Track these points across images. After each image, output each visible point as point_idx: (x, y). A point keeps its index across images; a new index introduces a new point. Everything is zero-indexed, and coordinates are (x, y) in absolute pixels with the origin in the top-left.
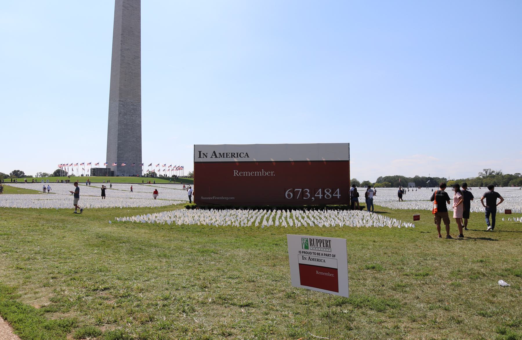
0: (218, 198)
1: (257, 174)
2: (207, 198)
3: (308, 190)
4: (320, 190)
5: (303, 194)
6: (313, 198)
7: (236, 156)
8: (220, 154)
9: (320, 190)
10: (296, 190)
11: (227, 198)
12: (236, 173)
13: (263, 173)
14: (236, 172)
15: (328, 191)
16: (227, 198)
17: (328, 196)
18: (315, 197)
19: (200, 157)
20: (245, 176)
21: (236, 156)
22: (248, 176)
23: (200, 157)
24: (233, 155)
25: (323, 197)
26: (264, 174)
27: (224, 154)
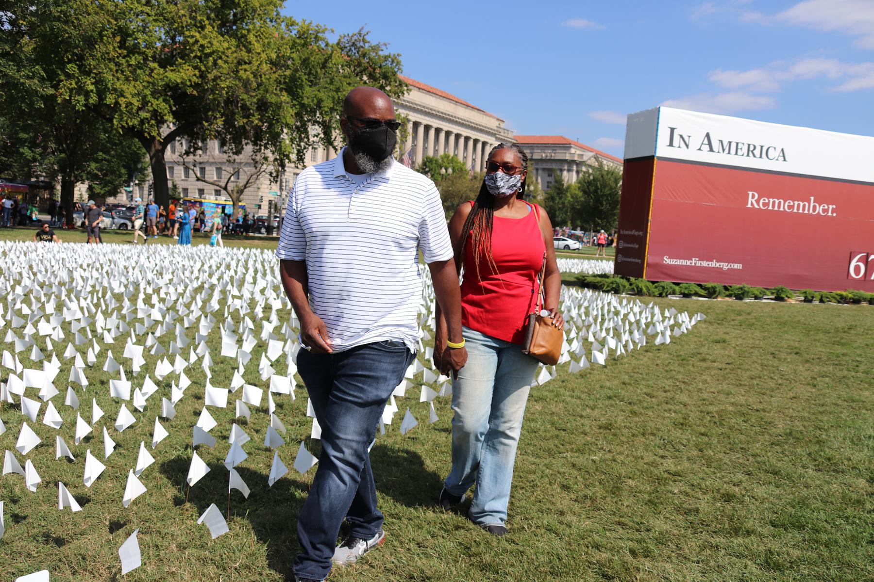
0: (705, 264)
2: (679, 262)
8: (721, 141)
11: (725, 266)
12: (752, 200)
14: (753, 196)
16: (725, 266)
19: (671, 144)
22: (778, 211)
23: (671, 144)
24: (750, 151)
26: (814, 208)
27: (730, 143)
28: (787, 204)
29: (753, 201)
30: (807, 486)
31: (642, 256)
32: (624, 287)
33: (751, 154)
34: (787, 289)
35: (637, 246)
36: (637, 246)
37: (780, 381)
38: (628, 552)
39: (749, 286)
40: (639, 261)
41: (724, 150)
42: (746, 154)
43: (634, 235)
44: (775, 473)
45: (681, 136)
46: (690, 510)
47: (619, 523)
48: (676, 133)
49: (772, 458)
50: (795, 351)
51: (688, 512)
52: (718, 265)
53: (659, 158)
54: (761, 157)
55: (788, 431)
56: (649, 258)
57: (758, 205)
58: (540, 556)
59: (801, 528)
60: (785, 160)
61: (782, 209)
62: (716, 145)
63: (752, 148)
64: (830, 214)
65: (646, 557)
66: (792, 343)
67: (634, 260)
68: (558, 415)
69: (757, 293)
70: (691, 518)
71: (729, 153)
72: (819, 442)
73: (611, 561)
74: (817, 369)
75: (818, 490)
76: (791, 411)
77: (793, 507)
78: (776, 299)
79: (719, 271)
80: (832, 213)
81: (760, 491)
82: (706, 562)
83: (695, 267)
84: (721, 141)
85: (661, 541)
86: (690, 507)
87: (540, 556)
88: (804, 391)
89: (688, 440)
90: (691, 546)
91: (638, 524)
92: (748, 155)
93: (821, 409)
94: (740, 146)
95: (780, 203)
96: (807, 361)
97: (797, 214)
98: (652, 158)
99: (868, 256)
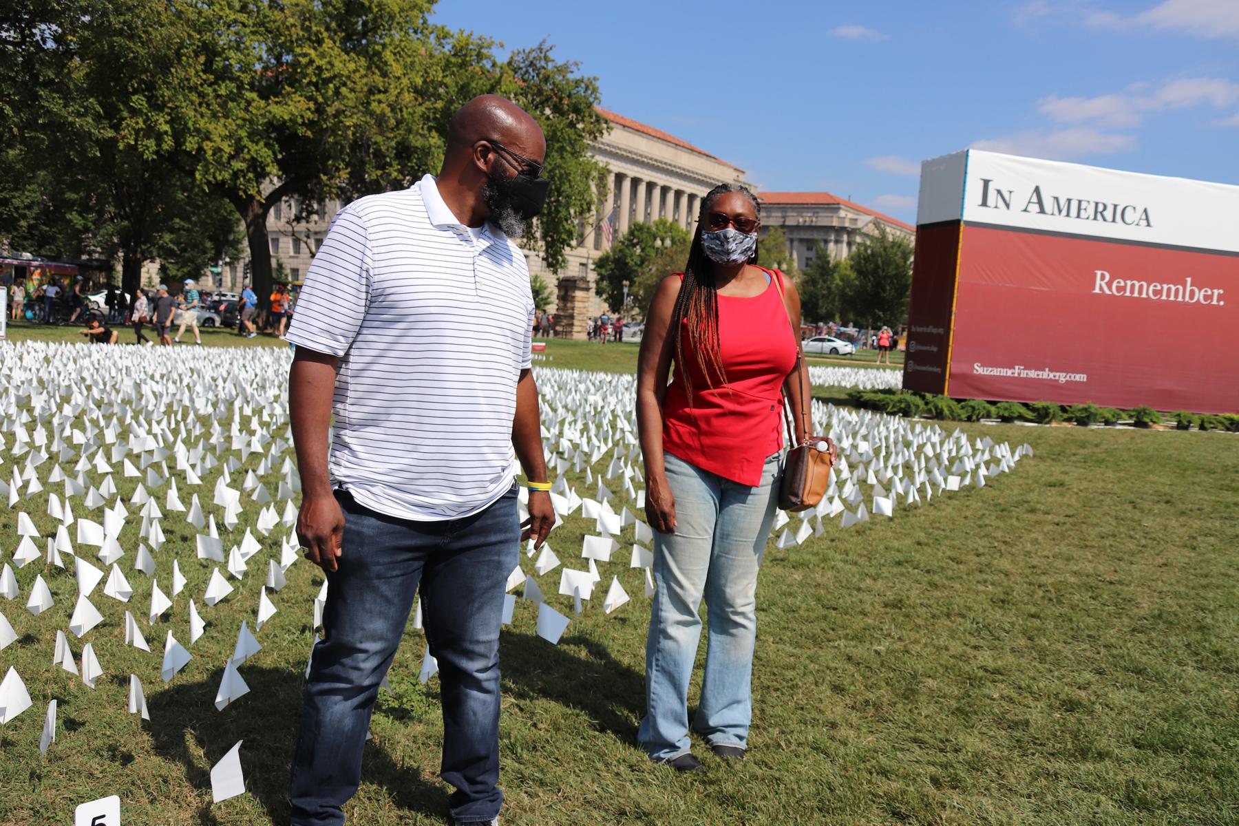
0: (1033, 374)
2: (996, 372)
7: (1108, 214)
8: (1057, 199)
11: (1062, 377)
12: (1102, 283)
13: (1189, 293)
14: (1103, 278)
16: (1062, 377)
19: (984, 203)
21: (1108, 214)
23: (984, 203)
24: (1099, 212)
27: (1069, 201)
28: (1151, 288)
30: (1186, 691)
31: (943, 365)
32: (917, 407)
33: (1099, 216)
34: (1153, 410)
35: (935, 349)
36: (935, 349)
37: (1143, 542)
38: (928, 781)
39: (1096, 406)
40: (939, 370)
41: (1060, 211)
42: (1092, 217)
43: (931, 334)
44: (1139, 672)
45: (999, 192)
46: (1016, 723)
47: (915, 740)
49: (1134, 650)
50: (1165, 498)
51: (1014, 725)
52: (1051, 376)
53: (967, 223)
54: (1114, 221)
55: (1156, 612)
56: (952, 366)
57: (1110, 288)
58: (804, 786)
59: (1177, 749)
60: (1149, 225)
61: (1144, 295)
63: (1100, 208)
64: (1215, 302)
65: (954, 788)
66: (1160, 488)
67: (931, 369)
68: (826, 588)
69: (1109, 416)
70: (1018, 734)
71: (1068, 215)
72: (1202, 628)
73: (904, 792)
74: (1197, 524)
75: (1202, 697)
76: (1160, 584)
77: (1166, 720)
78: (1135, 425)
79: (1054, 384)
80: (1218, 300)
81: (1118, 697)
82: (1041, 796)
83: (1019, 379)
84: (1057, 199)
85: (976, 765)
86: (1016, 718)
87: (804, 786)
88: (1179, 556)
89: (1013, 624)
90: (1018, 773)
91: (942, 741)
92: (1095, 218)
93: (1204, 581)
94: (1084, 205)
95: (1141, 287)
96: (1183, 513)
97: (1167, 302)
98: (955, 224)
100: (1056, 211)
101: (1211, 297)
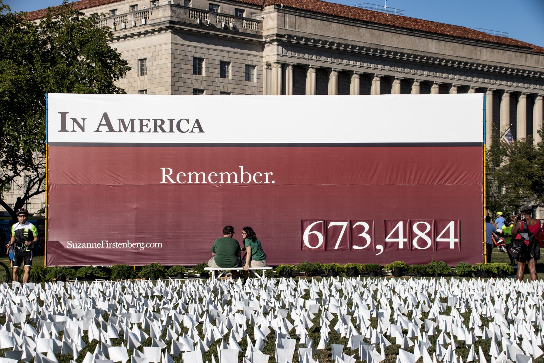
0: (117, 246)
1: (225, 178)
3: (366, 226)
4: (400, 225)
5: (353, 235)
6: (380, 247)
7: (166, 127)
8: (122, 121)
9: (400, 225)
10: (332, 224)
12: (166, 176)
14: (167, 172)
15: (422, 228)
17: (422, 242)
18: (385, 245)
19: (64, 128)
20: (193, 185)
21: (166, 127)
22: (201, 185)
23: (64, 128)
24: (158, 126)
25: (408, 245)
26: (246, 178)
27: (132, 121)
29: (168, 176)
33: (158, 129)
41: (126, 129)
42: (153, 130)
48: (68, 117)
54: (171, 131)
57: (175, 180)
60: (201, 131)
62: (116, 125)
63: (159, 123)
71: (133, 130)
80: (270, 180)
92: (156, 131)
94: (145, 122)
95: (201, 177)
99: (326, 223)
100: (122, 129)
101: (264, 178)
